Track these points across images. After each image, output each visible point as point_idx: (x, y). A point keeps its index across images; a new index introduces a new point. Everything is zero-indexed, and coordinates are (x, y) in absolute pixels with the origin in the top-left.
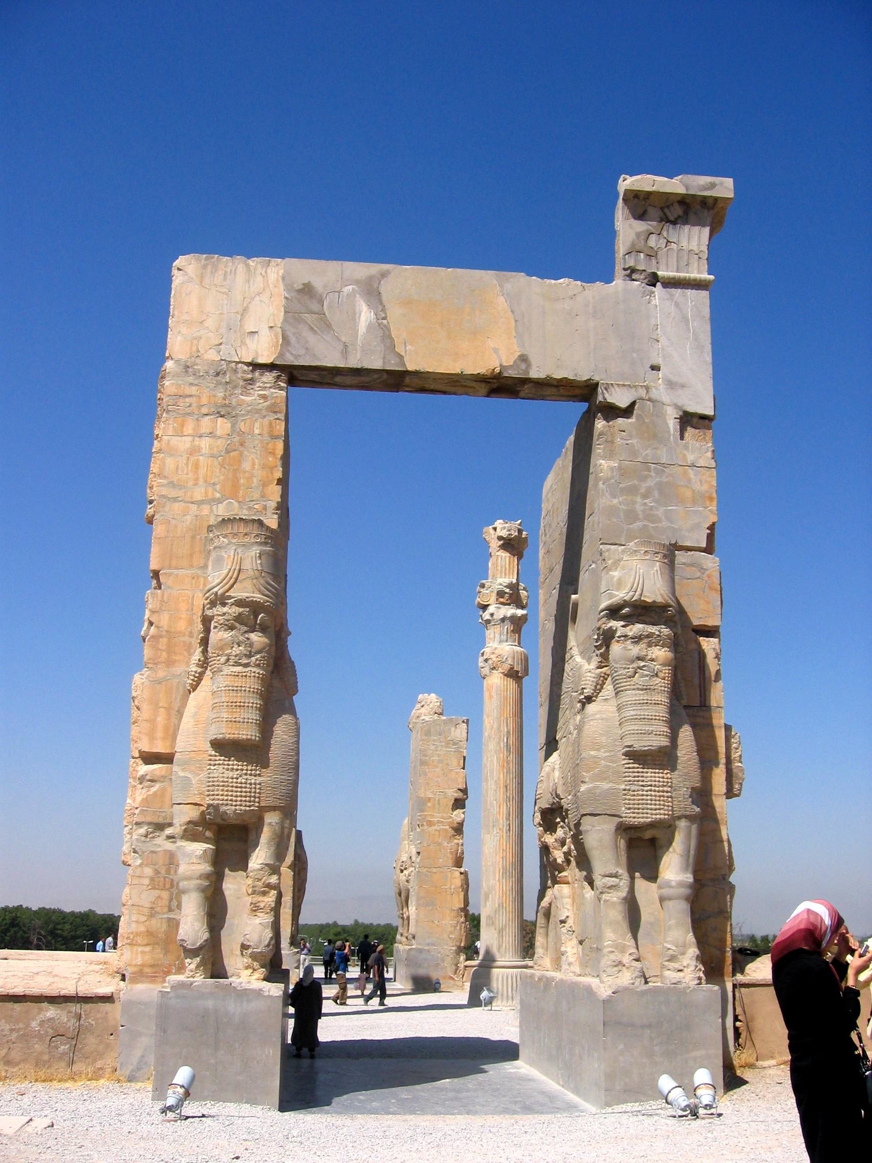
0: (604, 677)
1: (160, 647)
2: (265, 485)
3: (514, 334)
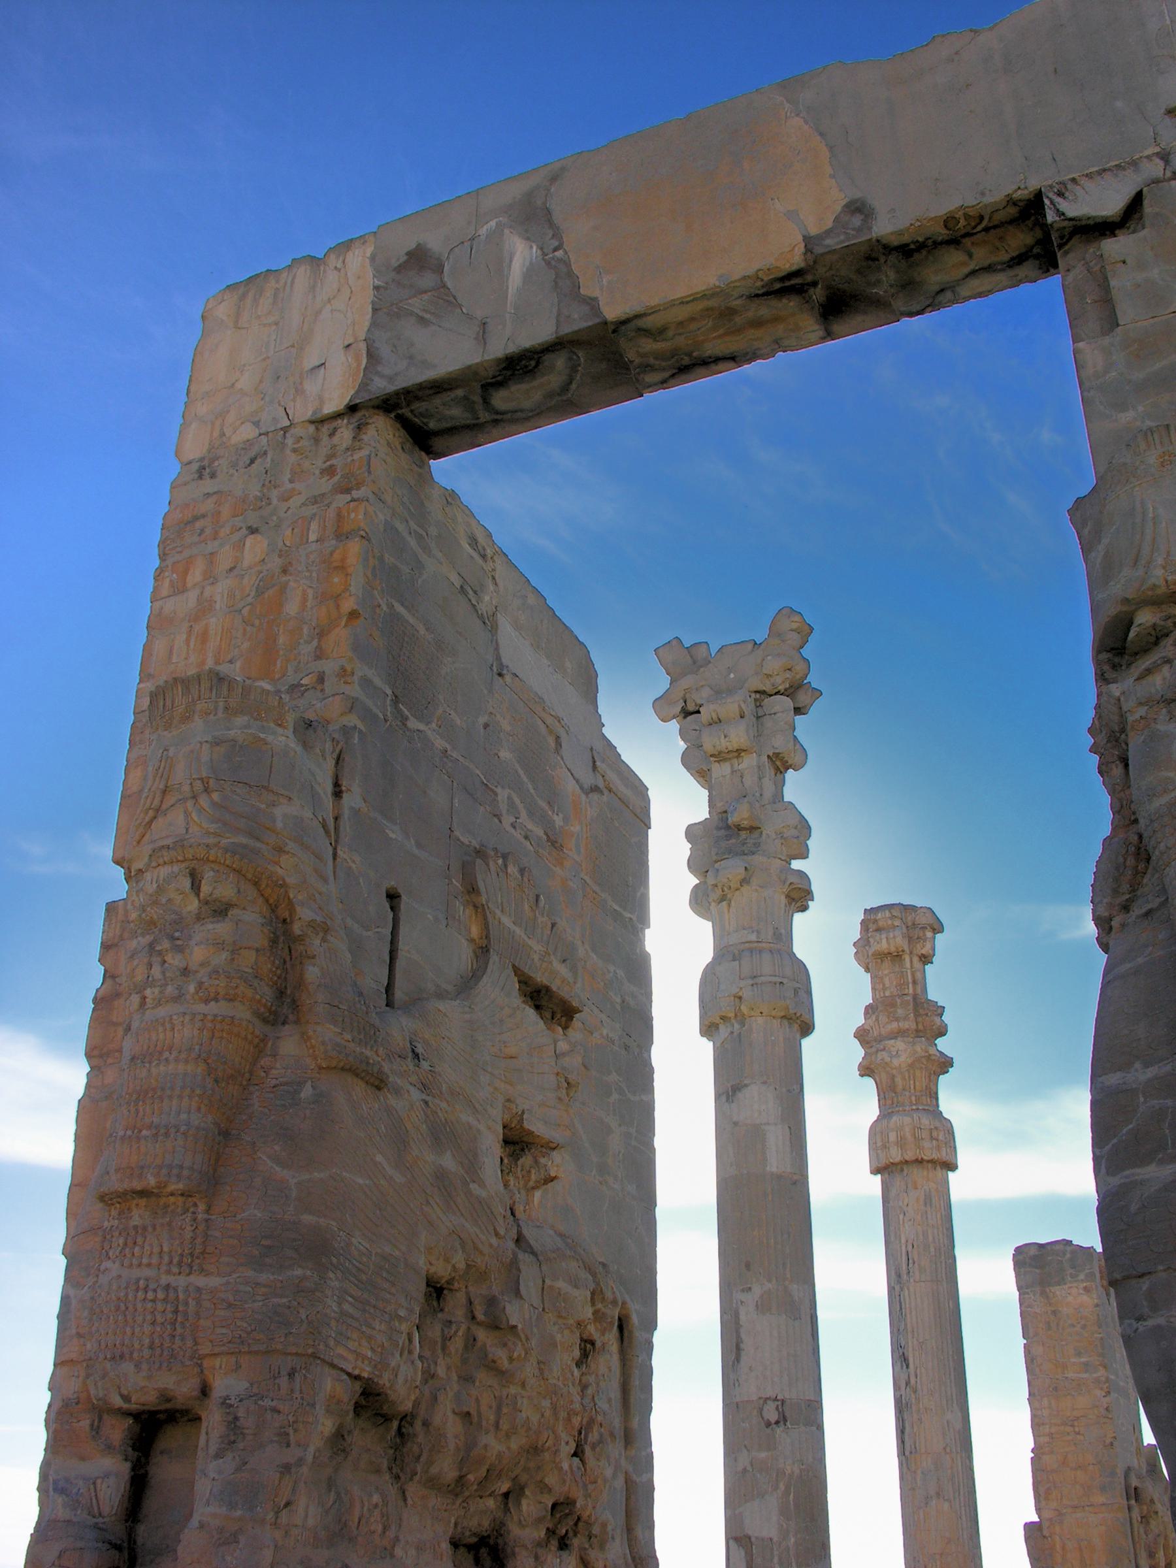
1: (115, 1020)
2: (322, 633)
3: (829, 170)
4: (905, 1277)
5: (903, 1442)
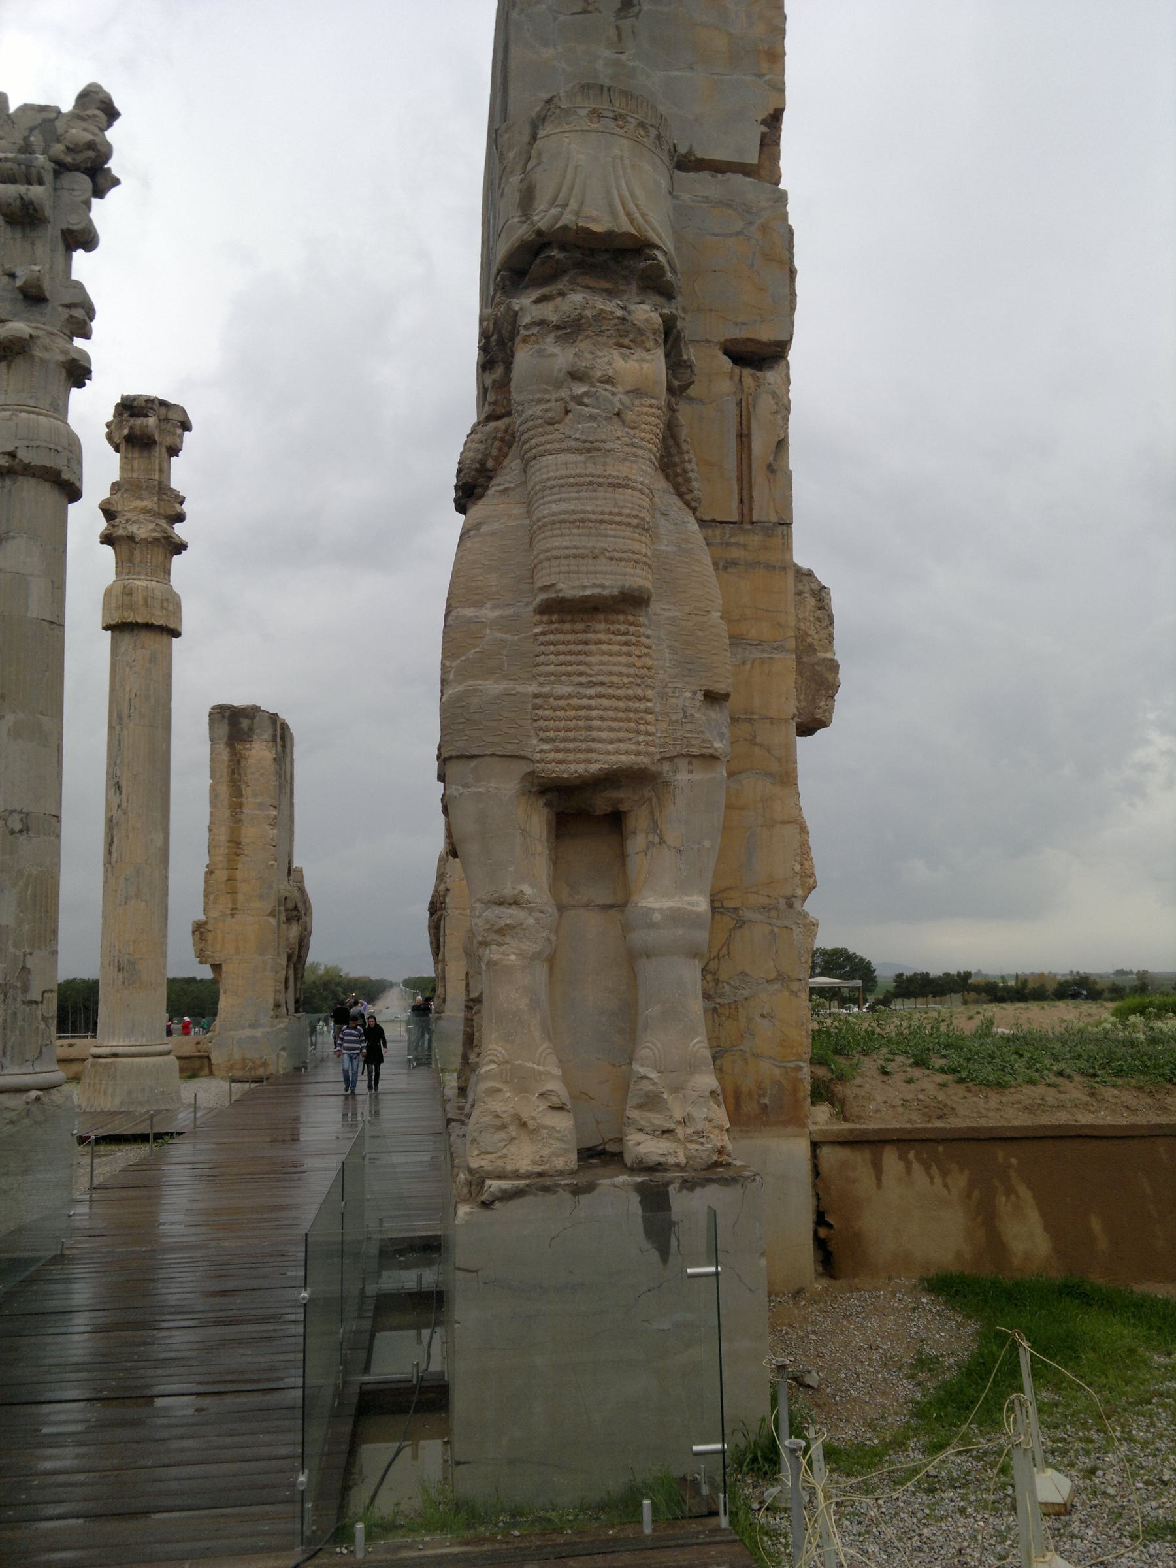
0: (502, 440)
4: (125, 720)
5: (110, 853)
